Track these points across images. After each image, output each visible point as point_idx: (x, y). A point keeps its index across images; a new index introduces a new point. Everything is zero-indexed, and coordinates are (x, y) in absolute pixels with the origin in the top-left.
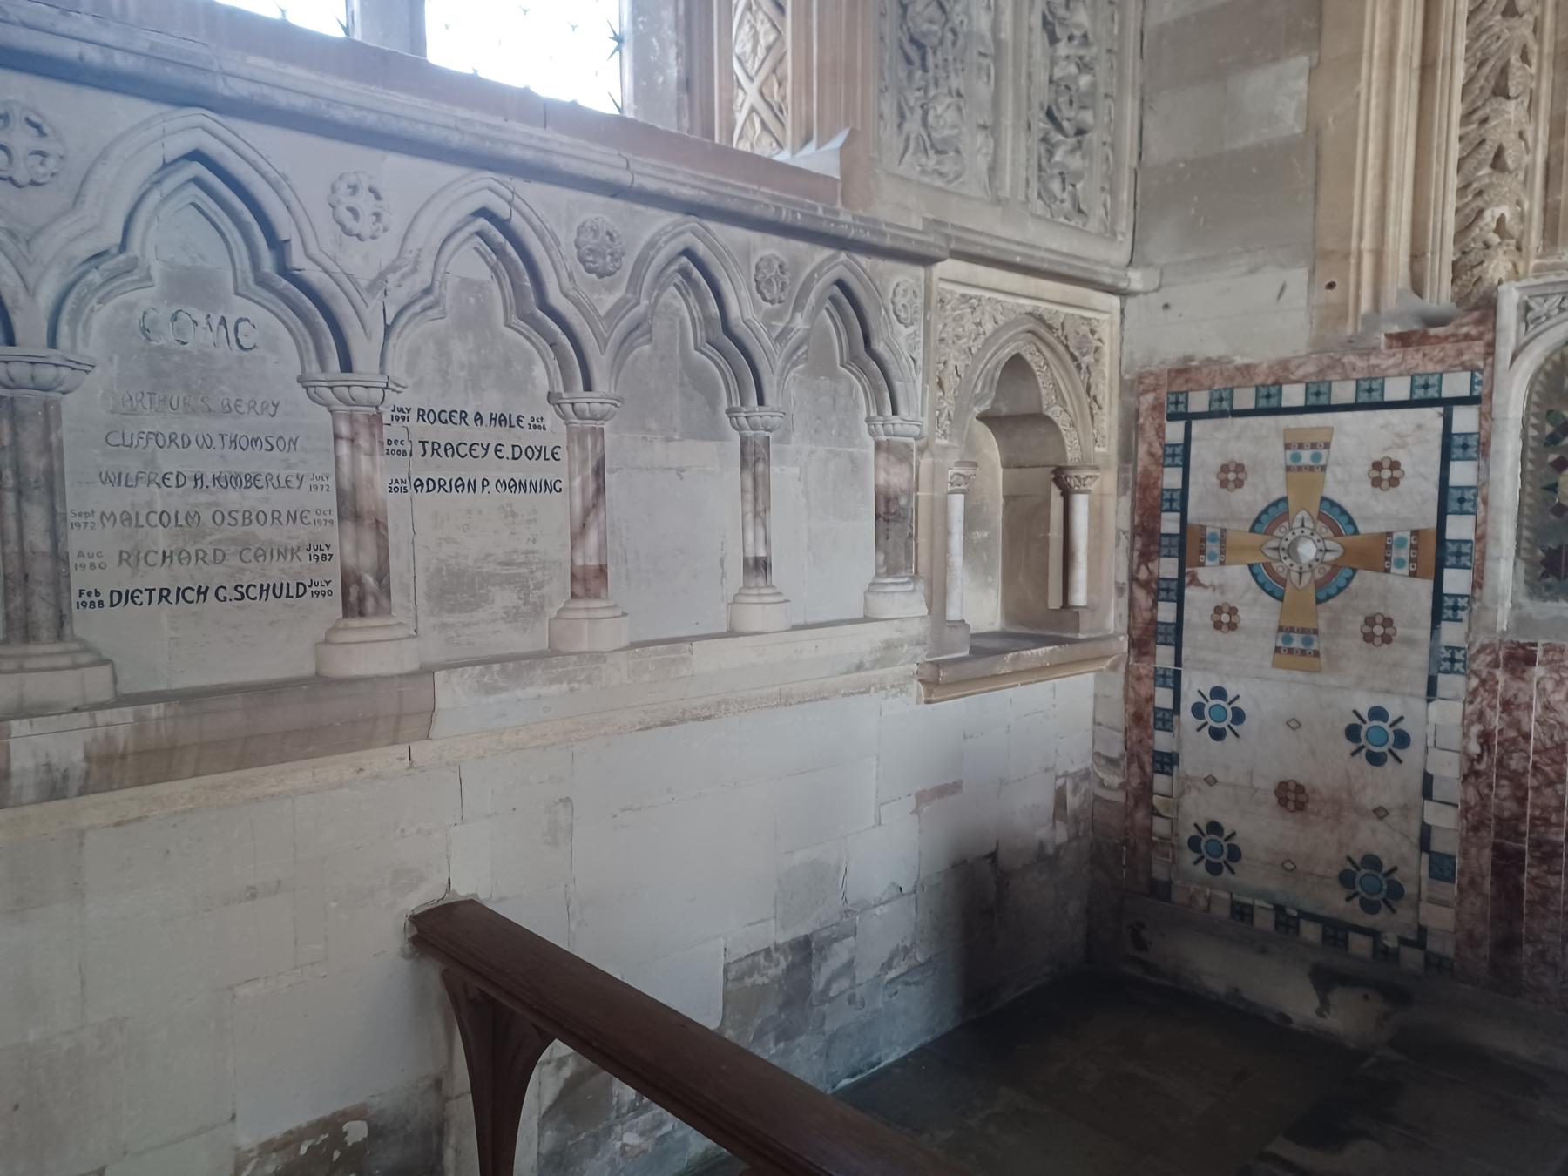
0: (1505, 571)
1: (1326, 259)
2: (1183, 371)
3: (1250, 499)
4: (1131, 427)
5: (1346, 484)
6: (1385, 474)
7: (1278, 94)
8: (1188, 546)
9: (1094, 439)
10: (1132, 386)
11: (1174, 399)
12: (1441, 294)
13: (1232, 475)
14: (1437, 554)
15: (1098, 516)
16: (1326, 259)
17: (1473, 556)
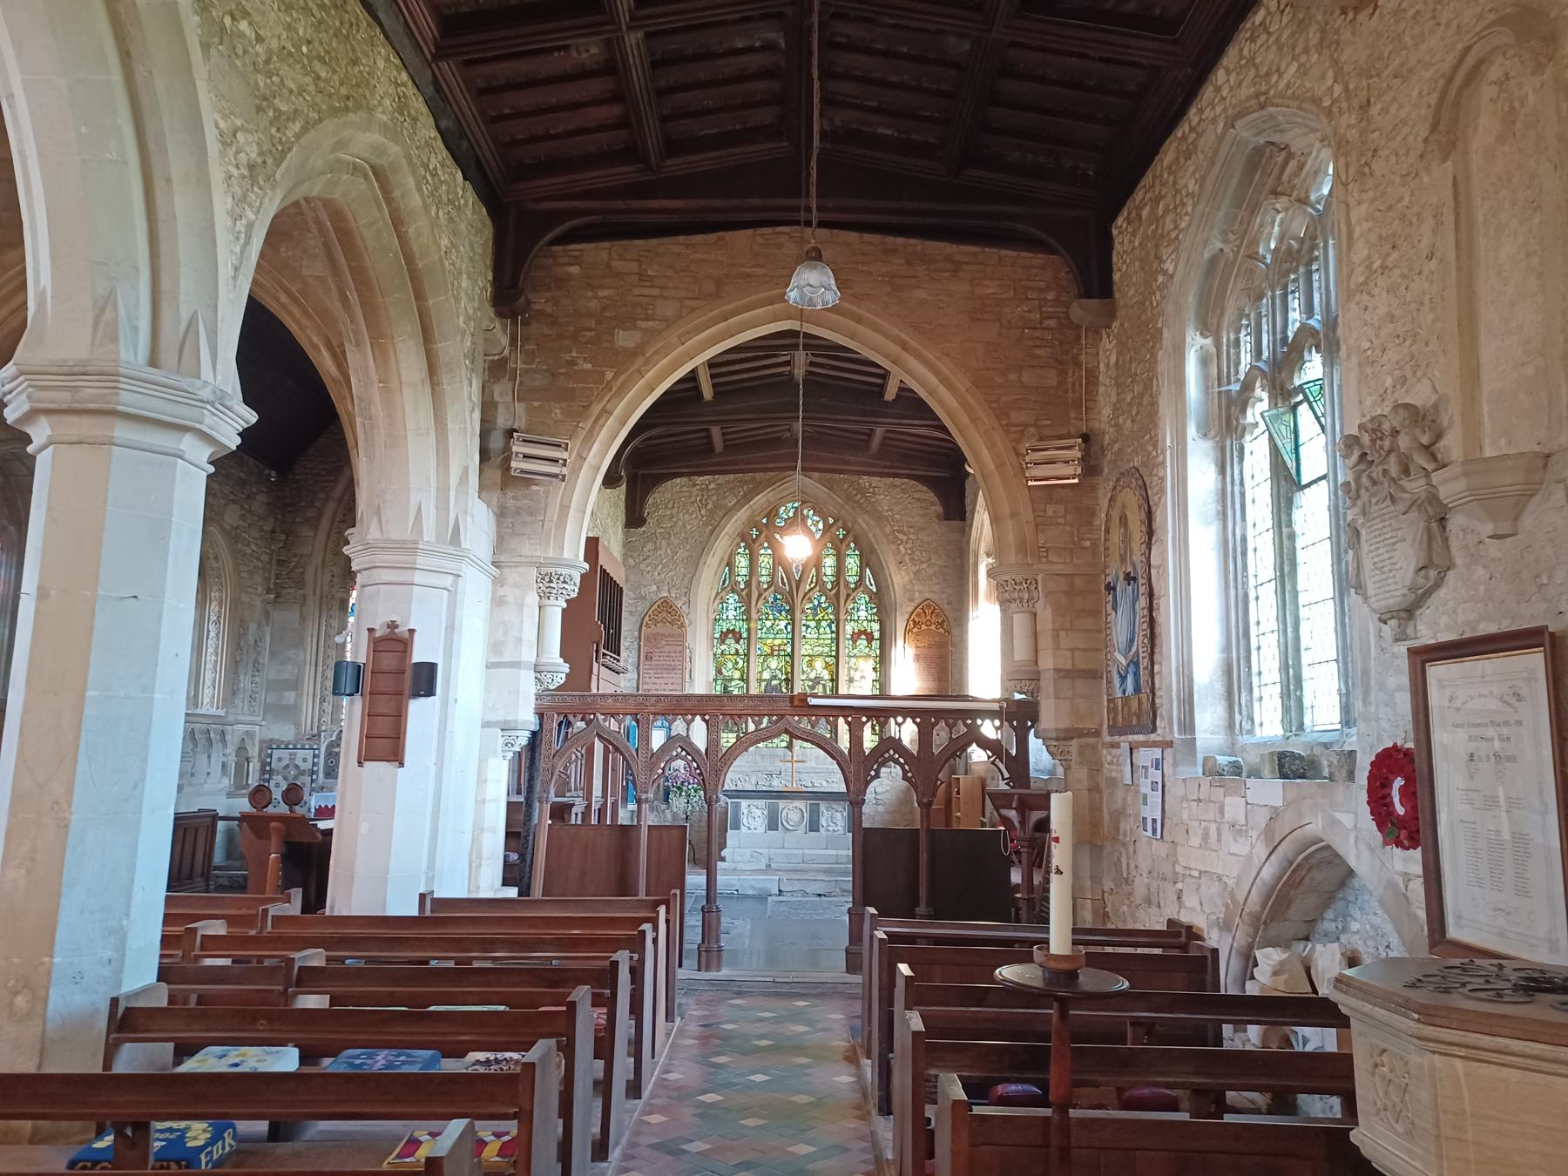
0: (321, 775)
1: (297, 725)
2: (272, 741)
3: (283, 764)
4: (261, 750)
5: (299, 762)
6: (305, 760)
7: (290, 697)
8: (271, 772)
9: (254, 752)
10: (262, 742)
11: (269, 745)
12: (315, 731)
13: (280, 759)
14: (312, 772)
15: (254, 766)
16: (297, 725)
17: (316, 773)
